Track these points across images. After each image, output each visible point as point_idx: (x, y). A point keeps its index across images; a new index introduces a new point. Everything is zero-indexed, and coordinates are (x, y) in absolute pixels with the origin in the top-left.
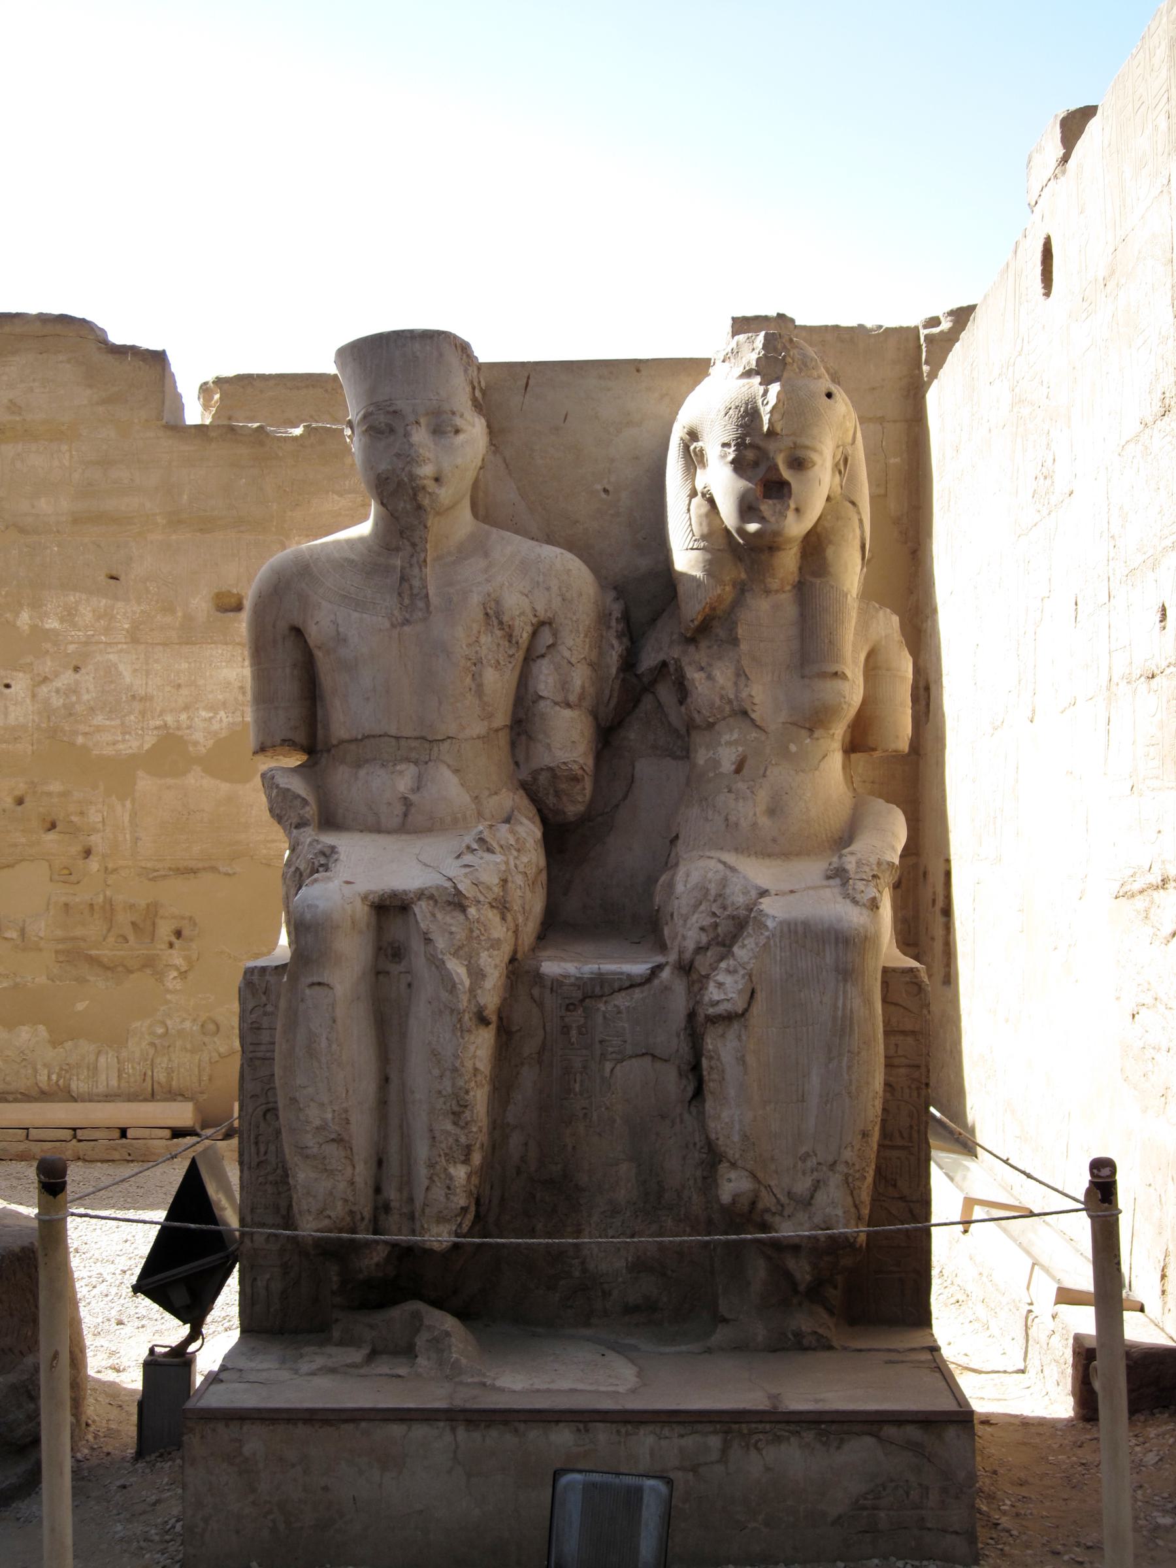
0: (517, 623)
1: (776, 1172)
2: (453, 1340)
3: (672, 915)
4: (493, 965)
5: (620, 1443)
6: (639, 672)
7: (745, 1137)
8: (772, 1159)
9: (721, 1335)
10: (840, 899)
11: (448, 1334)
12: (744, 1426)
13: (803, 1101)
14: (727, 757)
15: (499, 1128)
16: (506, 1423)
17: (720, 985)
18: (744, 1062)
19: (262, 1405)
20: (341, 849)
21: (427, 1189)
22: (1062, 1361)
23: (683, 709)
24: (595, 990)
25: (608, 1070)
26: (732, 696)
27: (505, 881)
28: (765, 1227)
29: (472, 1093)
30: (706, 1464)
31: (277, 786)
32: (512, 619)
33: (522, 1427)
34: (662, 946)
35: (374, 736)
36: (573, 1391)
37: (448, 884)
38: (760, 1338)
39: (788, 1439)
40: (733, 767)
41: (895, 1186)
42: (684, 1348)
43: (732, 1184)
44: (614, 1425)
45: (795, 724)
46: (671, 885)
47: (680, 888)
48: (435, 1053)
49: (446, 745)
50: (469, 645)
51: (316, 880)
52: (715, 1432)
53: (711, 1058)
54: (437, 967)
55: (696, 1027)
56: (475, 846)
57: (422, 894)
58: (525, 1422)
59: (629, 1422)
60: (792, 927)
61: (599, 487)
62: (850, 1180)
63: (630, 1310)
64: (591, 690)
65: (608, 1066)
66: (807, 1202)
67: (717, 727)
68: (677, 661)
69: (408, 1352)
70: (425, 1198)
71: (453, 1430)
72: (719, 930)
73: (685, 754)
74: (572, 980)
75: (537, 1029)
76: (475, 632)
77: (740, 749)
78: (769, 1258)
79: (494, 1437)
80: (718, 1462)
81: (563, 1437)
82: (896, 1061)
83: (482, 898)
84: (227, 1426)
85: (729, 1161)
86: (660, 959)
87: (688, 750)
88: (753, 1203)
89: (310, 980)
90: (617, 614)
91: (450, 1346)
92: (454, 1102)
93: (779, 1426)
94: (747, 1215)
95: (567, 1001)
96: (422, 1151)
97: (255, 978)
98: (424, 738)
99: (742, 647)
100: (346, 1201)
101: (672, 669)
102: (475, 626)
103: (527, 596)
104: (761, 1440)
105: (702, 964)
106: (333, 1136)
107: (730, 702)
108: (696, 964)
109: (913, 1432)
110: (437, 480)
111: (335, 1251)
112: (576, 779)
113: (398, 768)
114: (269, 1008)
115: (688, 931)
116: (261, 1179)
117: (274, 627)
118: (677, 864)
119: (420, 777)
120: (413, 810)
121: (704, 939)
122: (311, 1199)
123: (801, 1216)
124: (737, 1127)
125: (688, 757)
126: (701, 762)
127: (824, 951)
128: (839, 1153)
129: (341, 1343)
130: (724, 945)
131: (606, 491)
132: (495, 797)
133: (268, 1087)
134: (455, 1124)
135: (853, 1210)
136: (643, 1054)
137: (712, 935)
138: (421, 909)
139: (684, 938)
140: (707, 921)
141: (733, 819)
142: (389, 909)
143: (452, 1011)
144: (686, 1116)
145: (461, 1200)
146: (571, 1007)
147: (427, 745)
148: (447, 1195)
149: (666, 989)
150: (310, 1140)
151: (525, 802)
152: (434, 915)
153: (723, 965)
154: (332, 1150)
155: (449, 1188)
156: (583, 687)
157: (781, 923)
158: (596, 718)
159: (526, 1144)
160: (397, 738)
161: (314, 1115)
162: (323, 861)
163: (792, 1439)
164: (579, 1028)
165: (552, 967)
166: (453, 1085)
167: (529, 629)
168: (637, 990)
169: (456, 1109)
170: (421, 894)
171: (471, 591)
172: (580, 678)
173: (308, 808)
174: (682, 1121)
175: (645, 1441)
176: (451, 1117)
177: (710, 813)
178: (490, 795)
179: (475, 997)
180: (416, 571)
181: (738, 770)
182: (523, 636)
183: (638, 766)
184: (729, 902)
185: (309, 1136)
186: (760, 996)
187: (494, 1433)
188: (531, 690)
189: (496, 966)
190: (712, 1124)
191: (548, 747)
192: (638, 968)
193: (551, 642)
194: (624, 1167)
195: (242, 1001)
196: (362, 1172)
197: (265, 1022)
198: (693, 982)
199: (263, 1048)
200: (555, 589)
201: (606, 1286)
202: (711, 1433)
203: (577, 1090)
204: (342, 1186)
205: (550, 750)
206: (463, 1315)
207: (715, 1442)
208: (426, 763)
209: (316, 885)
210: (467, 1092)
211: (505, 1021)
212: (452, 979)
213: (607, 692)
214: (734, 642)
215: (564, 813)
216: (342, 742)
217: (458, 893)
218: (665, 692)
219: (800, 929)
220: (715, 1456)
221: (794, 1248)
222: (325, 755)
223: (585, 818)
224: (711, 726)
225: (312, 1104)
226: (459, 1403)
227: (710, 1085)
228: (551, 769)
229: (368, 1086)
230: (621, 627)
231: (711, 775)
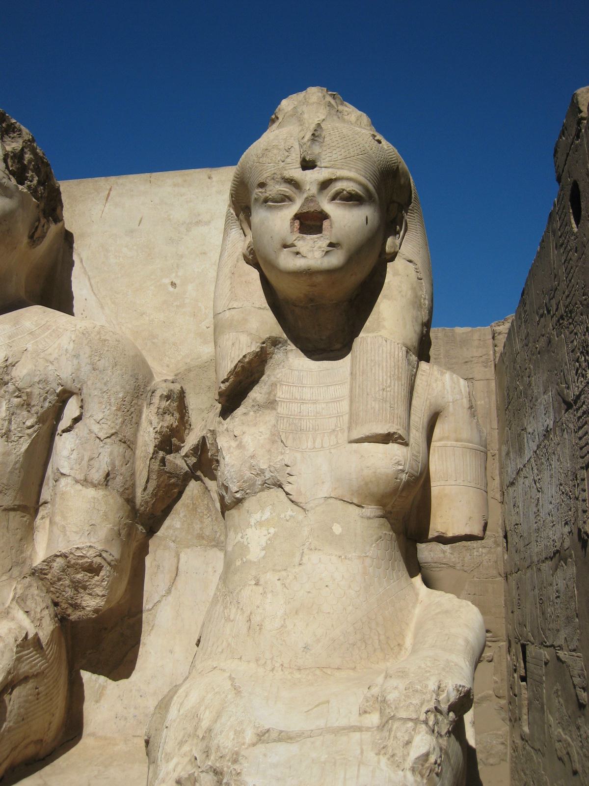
0: (36, 391)
61: (167, 281)
67: (246, 504)
77: (272, 530)
99: (279, 410)
131: (173, 284)
141: (256, 619)
177: (234, 610)
182: (40, 405)
193: (77, 414)
205: (65, 535)
214: (271, 404)
224: (238, 502)
231: (238, 563)
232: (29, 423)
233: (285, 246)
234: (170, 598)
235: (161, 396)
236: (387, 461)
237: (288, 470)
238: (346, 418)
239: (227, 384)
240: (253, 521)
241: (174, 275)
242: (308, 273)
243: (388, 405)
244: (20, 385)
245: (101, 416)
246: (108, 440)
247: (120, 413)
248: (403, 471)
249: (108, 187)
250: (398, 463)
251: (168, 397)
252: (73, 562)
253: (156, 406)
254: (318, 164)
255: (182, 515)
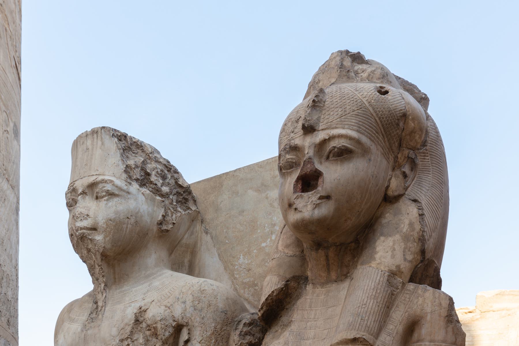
0: (159, 326)
102: (129, 329)
103: (169, 308)
200: (189, 303)
235: (244, 324)
239: (262, 312)
243: (360, 318)
244: (149, 322)
251: (250, 324)
253: (240, 330)
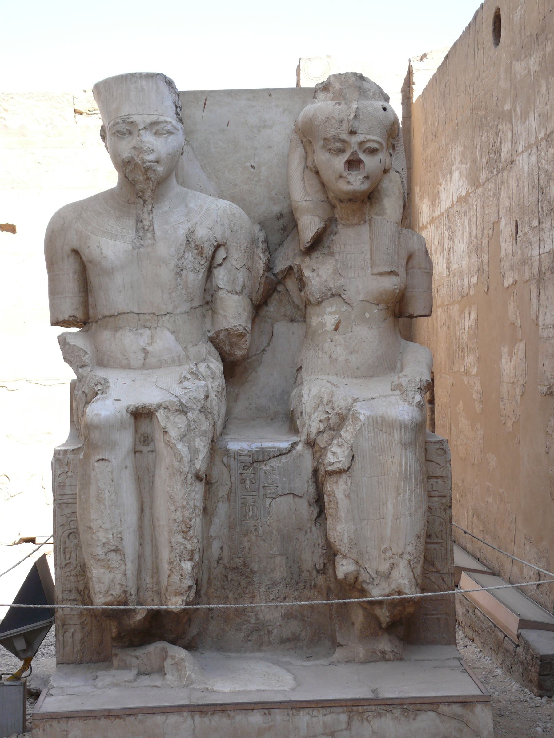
0: (206, 245)
1: (369, 560)
2: (187, 663)
3: (302, 413)
4: (202, 445)
5: (289, 720)
6: (275, 273)
7: (351, 540)
8: (367, 552)
9: (339, 654)
10: (400, 402)
11: (183, 660)
12: (360, 708)
13: (383, 518)
14: (330, 321)
15: (207, 540)
16: (223, 711)
17: (334, 453)
18: (350, 498)
19: (79, 708)
20: (110, 380)
21: (169, 576)
22: (525, 662)
23: (302, 293)
24: (259, 458)
25: (268, 503)
26: (332, 286)
27: (207, 397)
28: (363, 592)
29: (193, 520)
30: (338, 731)
31: (69, 344)
32: (203, 243)
33: (232, 713)
34: (294, 430)
35: (124, 313)
36: (258, 691)
37: (176, 400)
38: (361, 655)
39: (385, 715)
40: (333, 327)
41: (433, 565)
42: (317, 662)
43: (344, 568)
44: (286, 710)
45: (368, 301)
46: (300, 396)
47: (305, 397)
48: (171, 497)
49: (167, 317)
50: (179, 259)
51: (98, 399)
52: (344, 712)
53: (330, 495)
54: (171, 448)
55: (318, 477)
56: (189, 377)
57: (161, 405)
58: (234, 710)
59: (295, 708)
60: (375, 419)
61: (248, 164)
62: (412, 563)
63: (283, 641)
64: (248, 284)
65: (268, 501)
66: (387, 577)
67: (323, 304)
68: (298, 266)
69: (161, 671)
70: (168, 581)
71: (193, 717)
72: (331, 421)
73: (304, 319)
74: (246, 452)
75: (220, 479)
76: (182, 251)
77: (337, 316)
78: (365, 609)
79: (217, 720)
80: (346, 729)
81: (256, 719)
82: (432, 494)
83: (195, 407)
84: (59, 722)
85: (342, 554)
86: (295, 439)
87: (305, 317)
88: (357, 578)
89: (98, 458)
90: (262, 239)
91: (185, 667)
92: (184, 525)
93: (380, 707)
94: (353, 586)
95: (244, 465)
96: (165, 554)
97: (61, 456)
98: (153, 314)
100: (122, 585)
101: (295, 270)
102: (182, 248)
104: (370, 716)
105: (322, 442)
106: (114, 548)
107: (330, 289)
108: (318, 441)
109: (457, 709)
110: (157, 162)
111: (115, 615)
112: (242, 335)
113: (140, 331)
114: (70, 474)
115: (312, 423)
116: (67, 574)
117: (62, 249)
118: (302, 383)
119: (152, 336)
120: (149, 355)
121: (322, 427)
122: (101, 585)
123: (384, 585)
124: (346, 534)
125: (305, 322)
126: (314, 324)
127: (393, 432)
128: (405, 547)
129: (119, 668)
130: (334, 430)
131: (252, 166)
132: (196, 347)
133: (70, 519)
134: (184, 538)
135: (414, 580)
136: (288, 494)
137: (326, 425)
138: (160, 415)
139: (310, 426)
140: (325, 416)
141: (334, 357)
142: (141, 415)
143: (181, 473)
144: (314, 528)
145: (188, 582)
146: (246, 468)
147: (156, 318)
148: (181, 579)
149: (300, 456)
150: (100, 551)
151: (213, 349)
152: (168, 418)
153: (335, 442)
154: (113, 556)
155: (182, 576)
156: (244, 282)
157: (368, 417)
158: (251, 299)
159: (221, 548)
160: (138, 314)
161: (102, 536)
162: (100, 387)
163: (388, 715)
164: (251, 480)
165: (234, 446)
166: (183, 516)
167: (213, 249)
168: (284, 457)
169: (184, 529)
170: (159, 406)
171: (179, 227)
172: (241, 277)
173: (87, 356)
174: (311, 531)
175: (304, 719)
176: (182, 534)
177: (320, 353)
178: (193, 346)
179: (194, 464)
180: (146, 215)
181: (336, 329)
183: (275, 326)
184: (336, 405)
185: (99, 548)
186: (357, 459)
187: (216, 718)
188: (214, 284)
189: (205, 446)
190: (331, 534)
191: (225, 317)
192: (284, 445)
194: (278, 559)
195: (54, 470)
196: (131, 568)
197: (68, 482)
198: (316, 452)
199: (67, 497)
200: (226, 225)
201: (270, 628)
202: (341, 712)
203: (250, 515)
204: (119, 577)
205: (226, 319)
206: (189, 647)
207: (344, 718)
208: (156, 328)
209: (99, 402)
210: (191, 520)
211: (208, 477)
212: (180, 454)
213: (258, 285)
215: (235, 355)
216: (105, 317)
217: (181, 404)
218: (291, 284)
219: (379, 420)
220: (344, 726)
221: (380, 603)
222: (94, 324)
223: (246, 358)
224: (319, 303)
225: (100, 529)
226: (195, 701)
227: (330, 509)
228: (227, 330)
229: (131, 518)
230: (264, 246)
231: (320, 331)
232: (202, 263)
233: (341, 177)
234: (269, 348)
236: (390, 284)
237: (344, 288)
238: (369, 261)
239: (310, 244)
240: (327, 312)
241: (252, 161)
242: (354, 192)
244: (198, 243)
245: (237, 256)
246: (241, 269)
247: (246, 254)
248: (397, 288)
249: (205, 98)
250: (395, 285)
252: (232, 333)
254: (358, 132)
255: (273, 304)
